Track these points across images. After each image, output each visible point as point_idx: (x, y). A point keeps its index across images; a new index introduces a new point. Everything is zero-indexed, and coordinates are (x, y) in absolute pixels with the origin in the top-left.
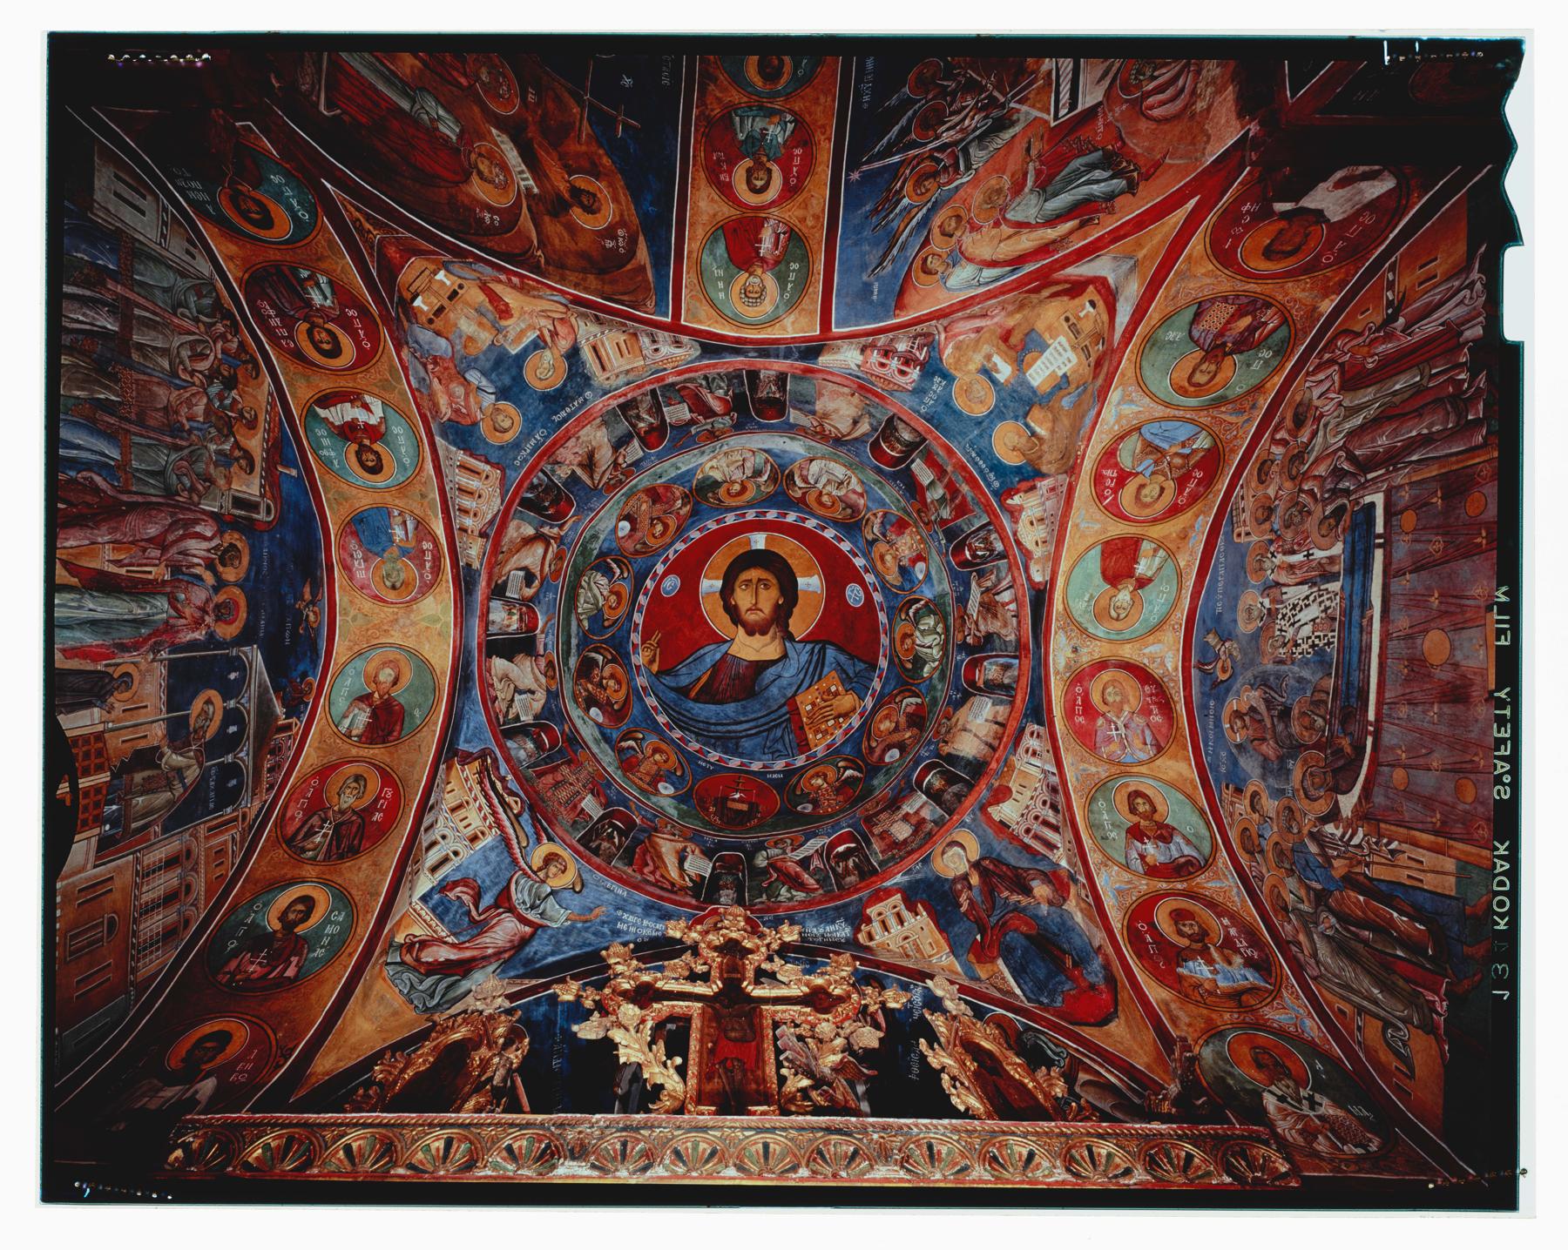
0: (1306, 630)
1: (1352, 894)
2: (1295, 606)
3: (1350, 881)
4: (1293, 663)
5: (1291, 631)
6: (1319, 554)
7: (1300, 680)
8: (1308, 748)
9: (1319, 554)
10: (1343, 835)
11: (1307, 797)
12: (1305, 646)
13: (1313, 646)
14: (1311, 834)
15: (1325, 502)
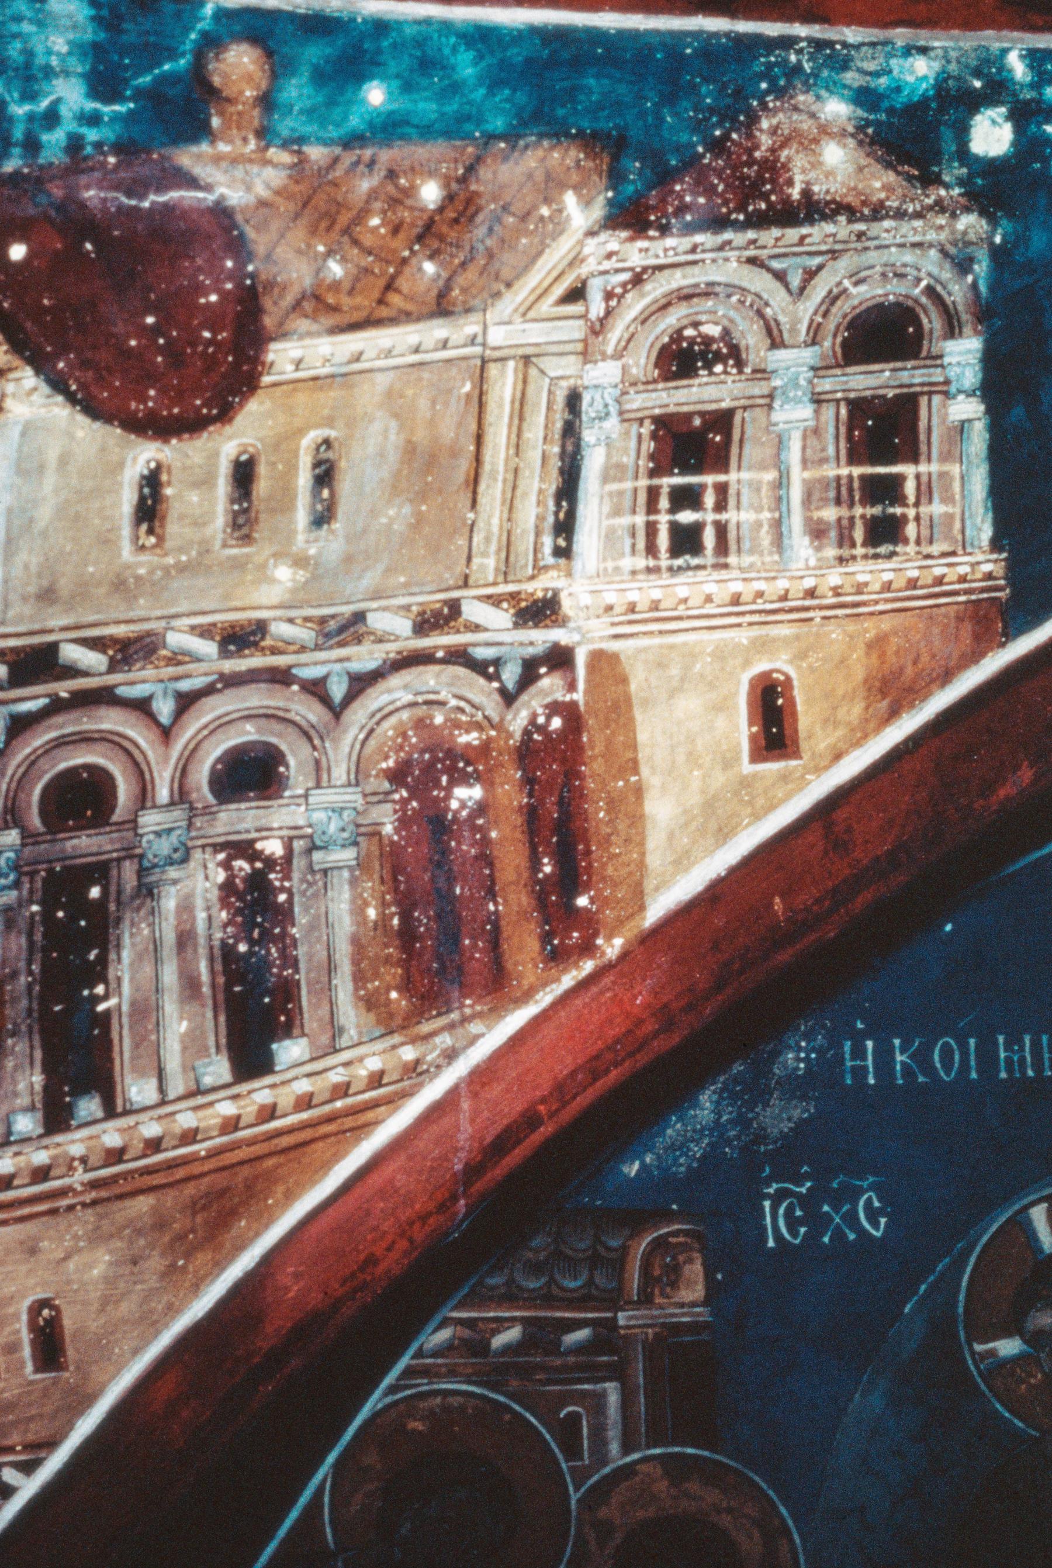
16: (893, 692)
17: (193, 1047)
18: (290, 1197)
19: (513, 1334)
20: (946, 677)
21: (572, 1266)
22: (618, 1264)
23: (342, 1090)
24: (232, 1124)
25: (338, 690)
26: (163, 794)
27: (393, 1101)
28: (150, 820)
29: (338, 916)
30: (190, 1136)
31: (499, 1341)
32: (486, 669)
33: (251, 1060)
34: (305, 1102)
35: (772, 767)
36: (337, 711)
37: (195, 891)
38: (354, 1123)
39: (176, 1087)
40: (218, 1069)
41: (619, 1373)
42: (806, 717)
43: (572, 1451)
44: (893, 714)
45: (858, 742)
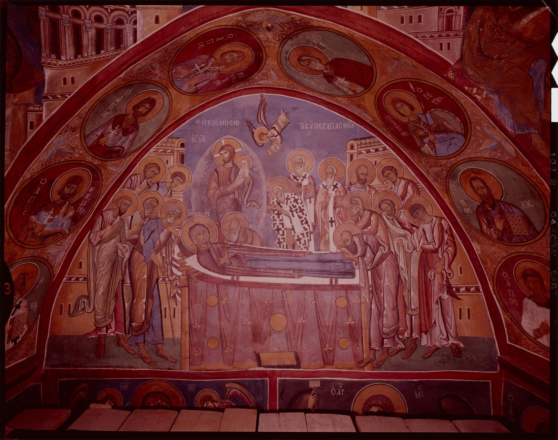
0: (288, 225)
1: (146, 269)
2: (302, 211)
3: (152, 266)
4: (268, 211)
5: (288, 209)
6: (331, 230)
7: (258, 219)
8: (219, 225)
9: (331, 230)
10: (175, 260)
11: (191, 229)
12: (278, 222)
13: (278, 229)
14: (170, 235)
15: (360, 236)
16: (169, 18)
17: (92, 51)
18: (101, 67)
19: (162, 150)
20: (175, 17)
21: (169, 143)
22: (174, 143)
23: (108, 56)
24: (96, 59)
25: (109, 11)
26: (88, 18)
27: (113, 58)
28: (86, 21)
29: (109, 37)
30: (91, 60)
31: (160, 151)
32: (127, 12)
33: (98, 52)
34: (104, 57)
35: (156, 25)
36: (110, 14)
37: (92, 33)
38: (110, 60)
39: (89, 54)
40: (94, 53)
41: (174, 155)
42: (160, 20)
43: (167, 163)
44: (169, 20)
45: (166, 23)
